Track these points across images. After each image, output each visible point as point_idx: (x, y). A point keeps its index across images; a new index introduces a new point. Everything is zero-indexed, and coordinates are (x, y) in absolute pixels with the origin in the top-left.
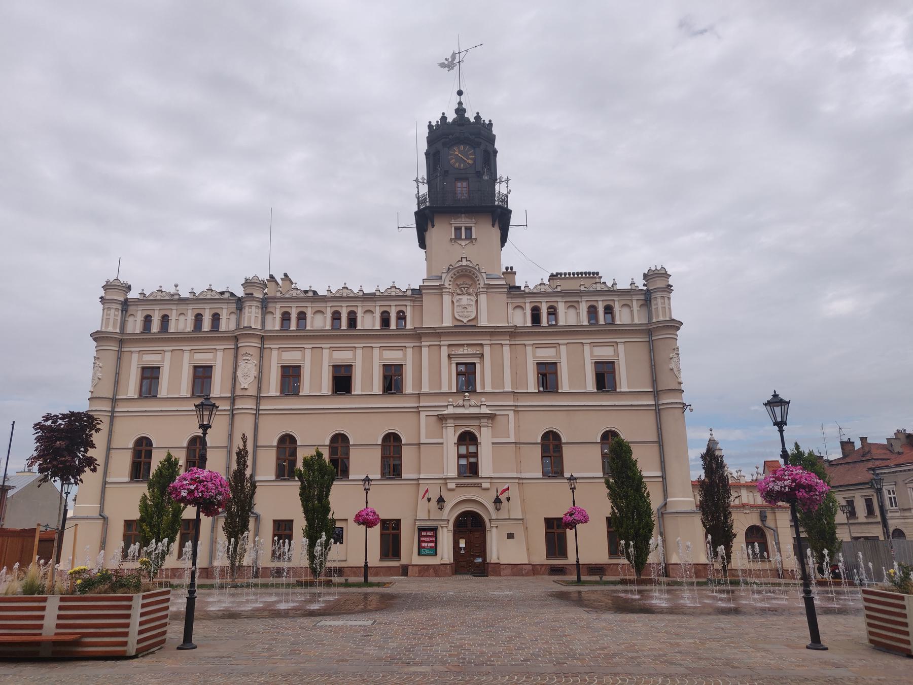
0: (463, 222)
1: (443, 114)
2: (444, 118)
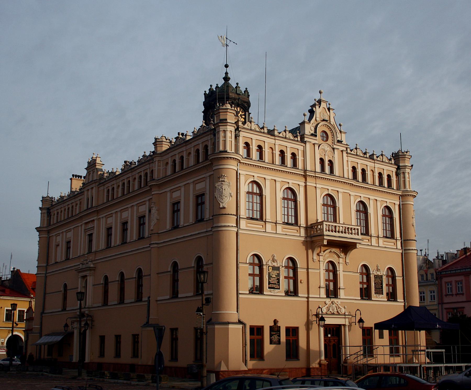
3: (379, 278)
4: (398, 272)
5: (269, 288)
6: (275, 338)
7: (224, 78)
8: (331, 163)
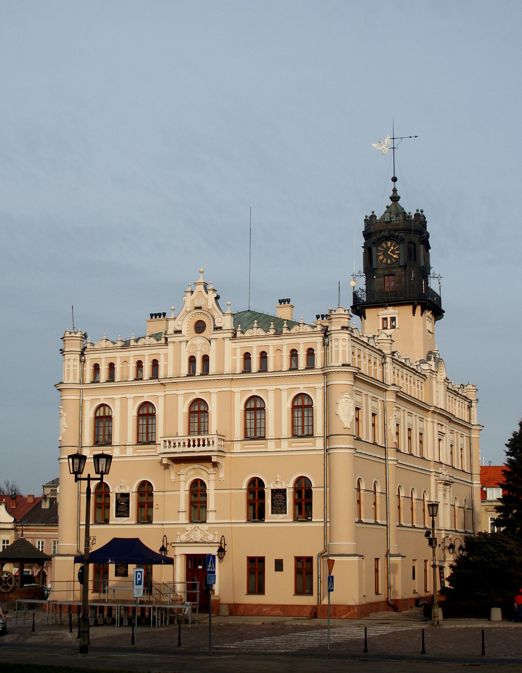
2: (373, 217)
3: (282, 493)
4: (316, 483)
5: (116, 516)
7: (391, 198)
8: (206, 359)
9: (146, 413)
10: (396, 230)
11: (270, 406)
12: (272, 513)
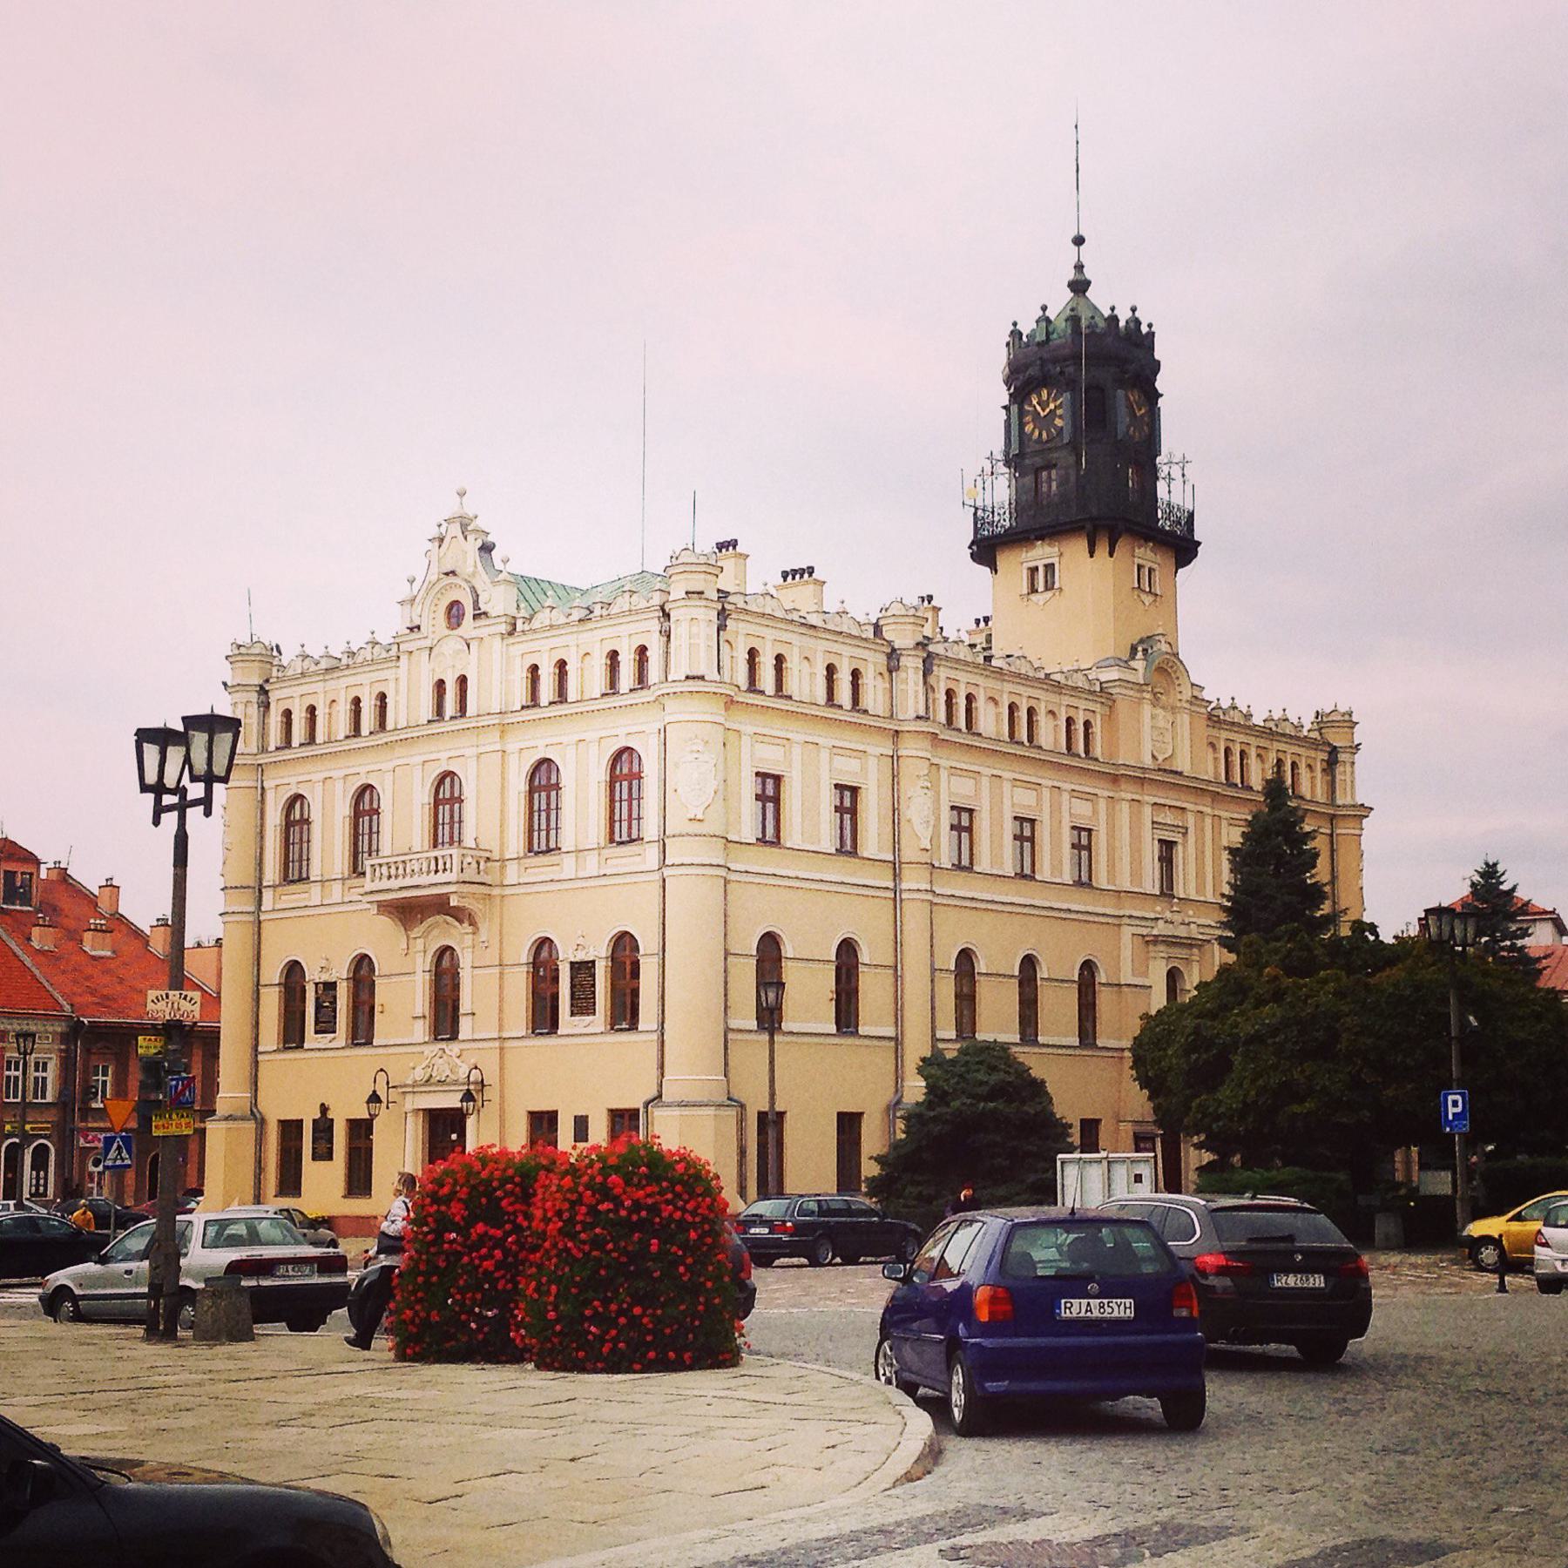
0: (1041, 553)
1: (1015, 324)
2: (1016, 334)
4: (647, 944)
6: (323, 1145)
9: (364, 805)
10: (1055, 361)
11: (567, 779)
12: (572, 1014)
